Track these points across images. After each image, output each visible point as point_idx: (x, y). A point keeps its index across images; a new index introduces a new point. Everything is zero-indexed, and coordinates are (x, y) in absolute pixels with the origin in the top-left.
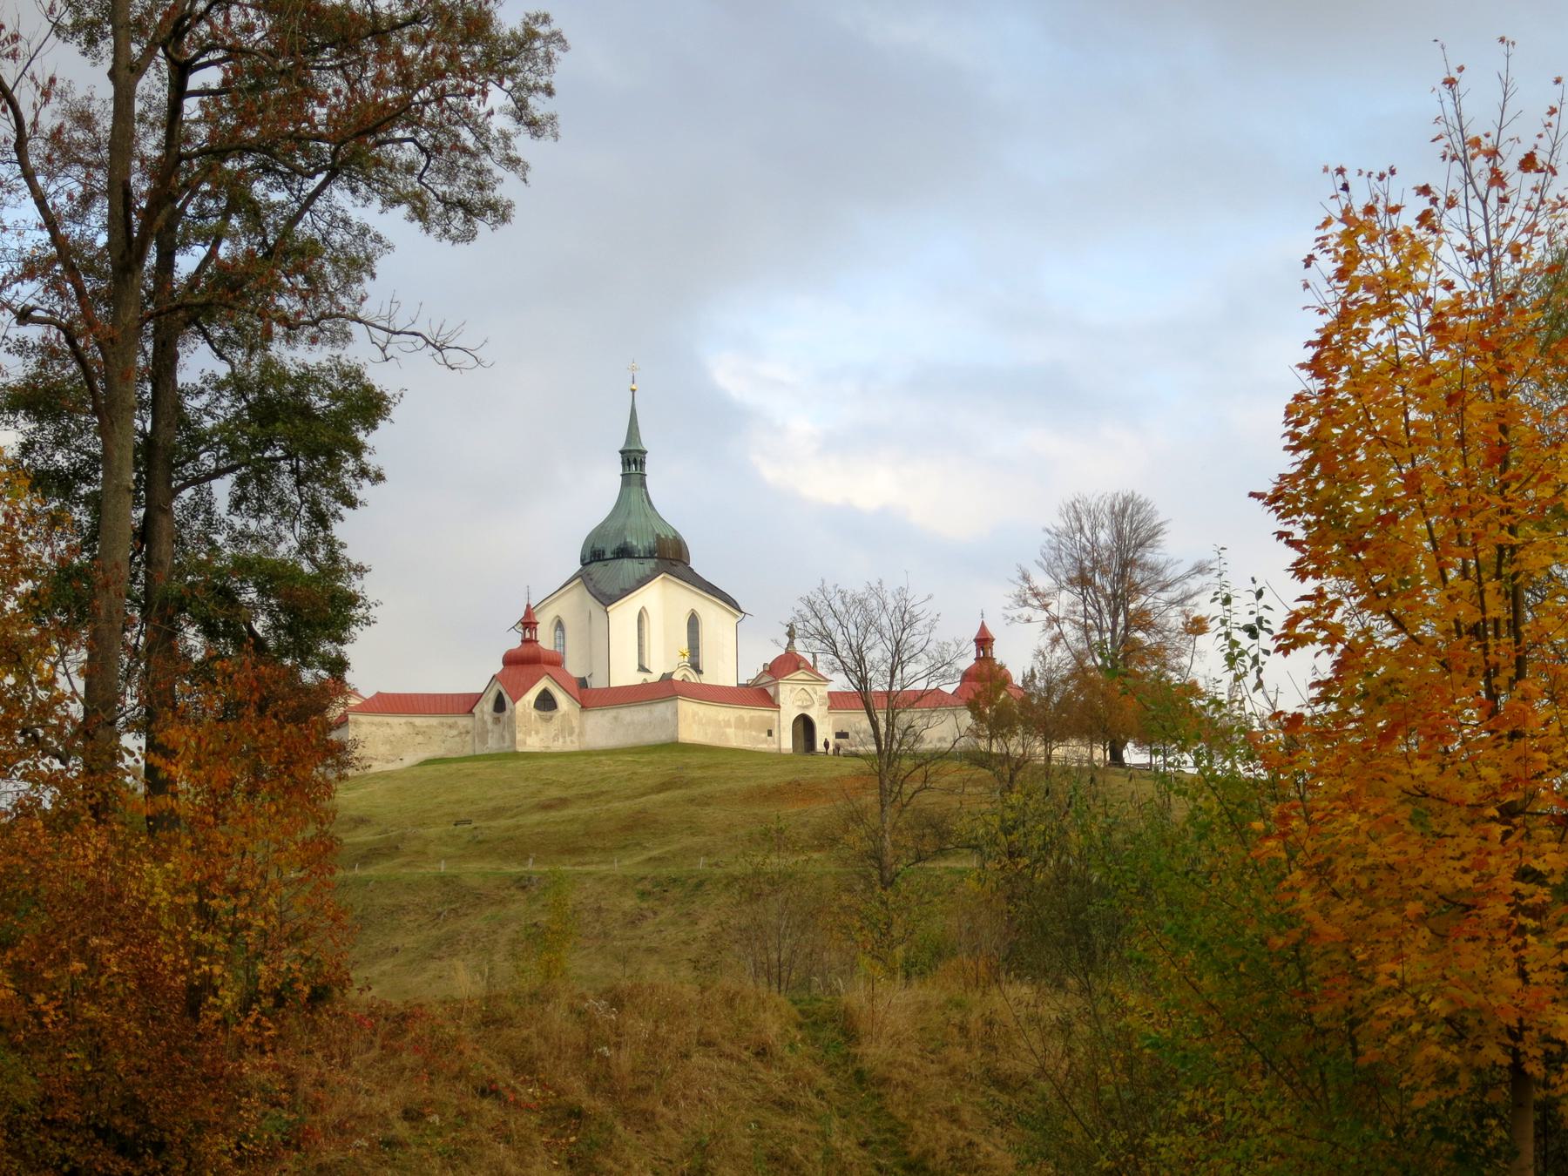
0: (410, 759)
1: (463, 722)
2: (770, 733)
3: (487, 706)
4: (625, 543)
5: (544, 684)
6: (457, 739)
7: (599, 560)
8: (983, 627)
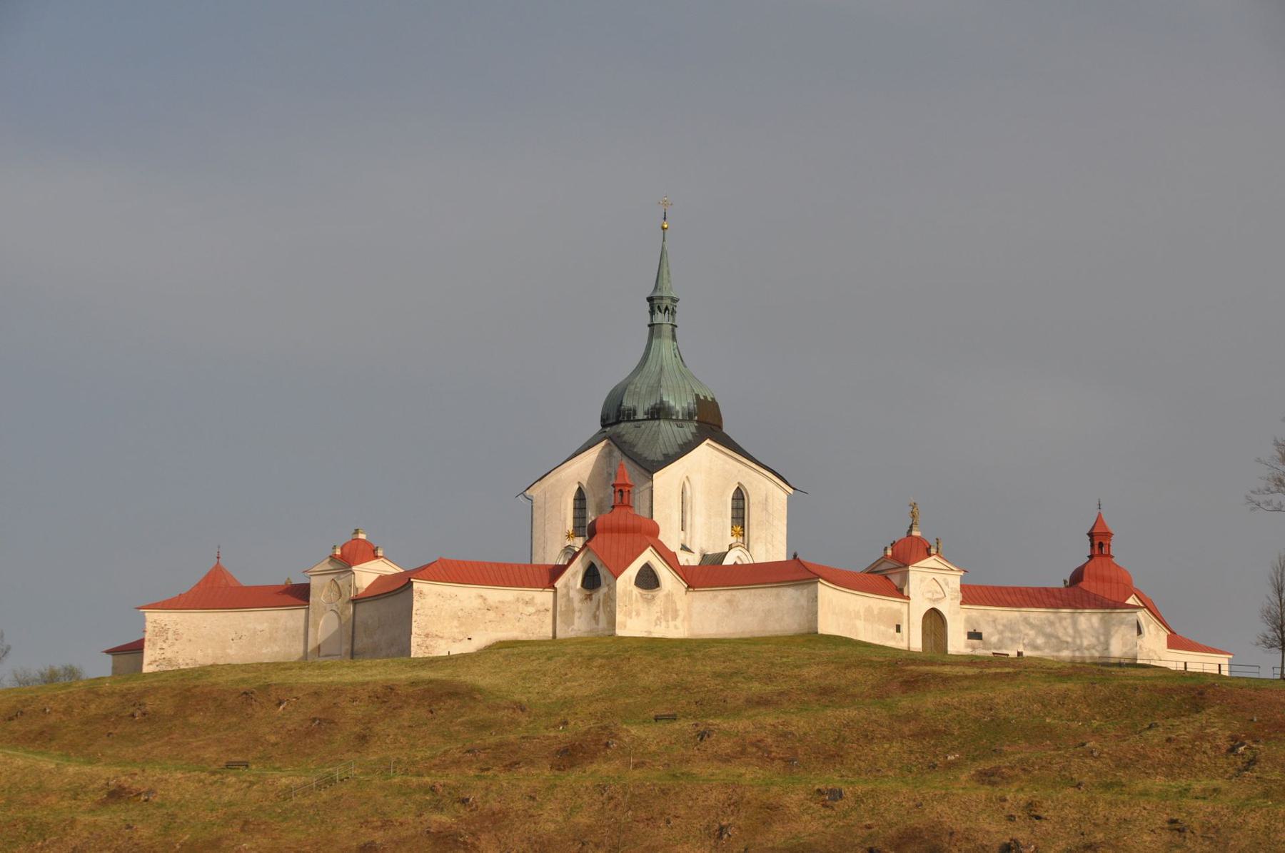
0: (480, 640)
1: (543, 597)
2: (898, 629)
3: (573, 578)
4: (662, 401)
5: (648, 556)
6: (534, 618)
7: (629, 421)
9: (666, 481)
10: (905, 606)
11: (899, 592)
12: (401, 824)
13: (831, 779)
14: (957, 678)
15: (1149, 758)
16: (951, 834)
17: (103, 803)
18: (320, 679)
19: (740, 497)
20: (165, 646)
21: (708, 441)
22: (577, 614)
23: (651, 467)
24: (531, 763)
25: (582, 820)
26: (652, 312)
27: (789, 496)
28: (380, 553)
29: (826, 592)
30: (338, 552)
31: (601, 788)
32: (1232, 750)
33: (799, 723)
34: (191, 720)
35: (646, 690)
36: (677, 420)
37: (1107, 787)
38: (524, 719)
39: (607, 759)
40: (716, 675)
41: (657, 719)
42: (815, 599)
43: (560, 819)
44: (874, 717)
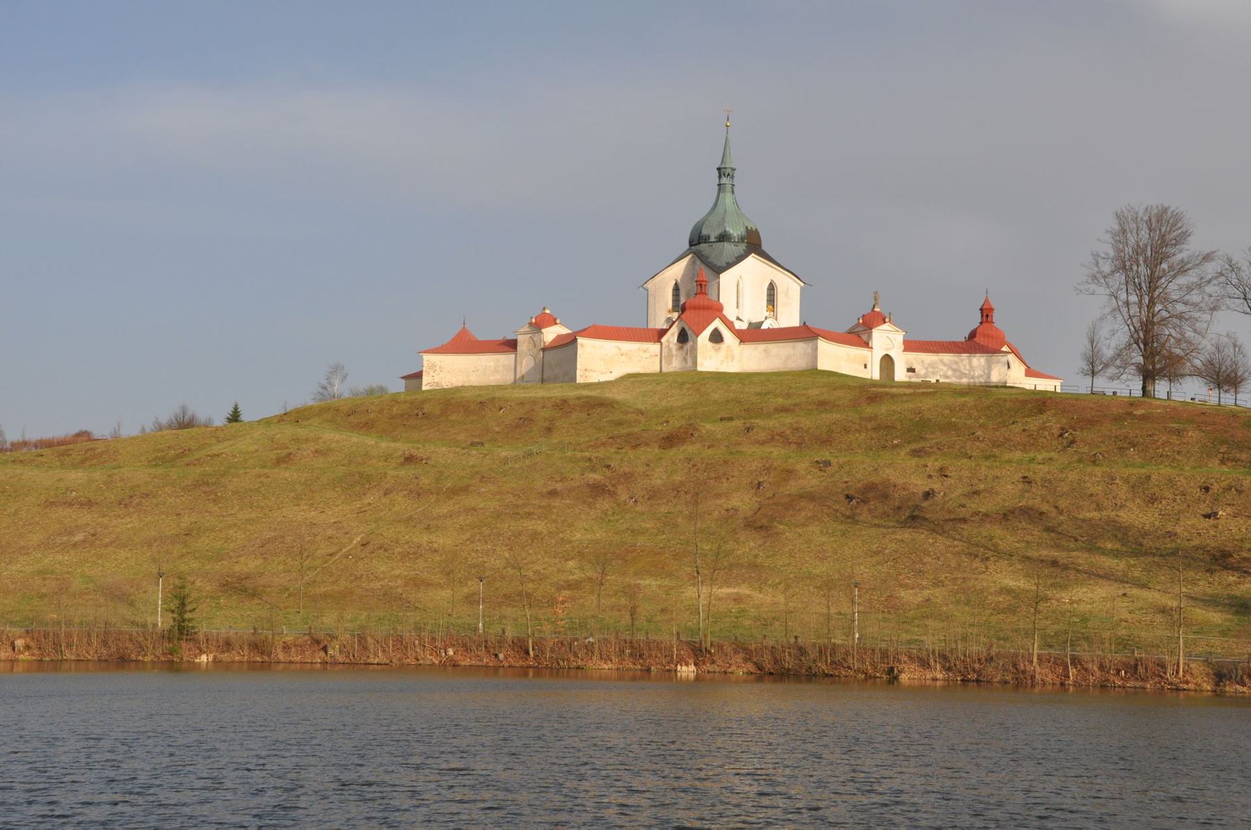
1: (654, 348)
2: (865, 366)
3: (672, 336)
4: (725, 231)
5: (717, 323)
7: (705, 242)
8: (986, 301)
9: (727, 278)
10: (869, 353)
11: (866, 345)
12: (572, 479)
13: (825, 454)
14: (899, 395)
15: (1012, 441)
16: (895, 486)
17: (402, 464)
18: (524, 395)
19: (772, 288)
20: (434, 374)
21: (753, 255)
22: (674, 358)
23: (718, 270)
24: (647, 444)
25: (678, 478)
26: (720, 177)
27: (801, 288)
28: (558, 321)
29: (822, 344)
30: (534, 321)
31: (689, 460)
32: (1061, 435)
33: (806, 422)
34: (450, 418)
35: (715, 402)
36: (735, 242)
37: (987, 458)
38: (643, 419)
39: (692, 443)
40: (758, 394)
41: (721, 420)
42: (816, 349)
43: (664, 477)
44: (850, 419)
